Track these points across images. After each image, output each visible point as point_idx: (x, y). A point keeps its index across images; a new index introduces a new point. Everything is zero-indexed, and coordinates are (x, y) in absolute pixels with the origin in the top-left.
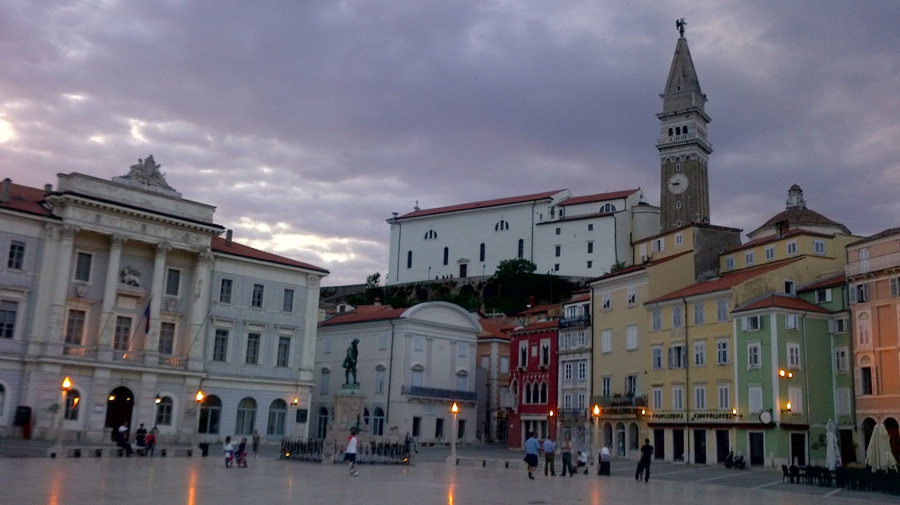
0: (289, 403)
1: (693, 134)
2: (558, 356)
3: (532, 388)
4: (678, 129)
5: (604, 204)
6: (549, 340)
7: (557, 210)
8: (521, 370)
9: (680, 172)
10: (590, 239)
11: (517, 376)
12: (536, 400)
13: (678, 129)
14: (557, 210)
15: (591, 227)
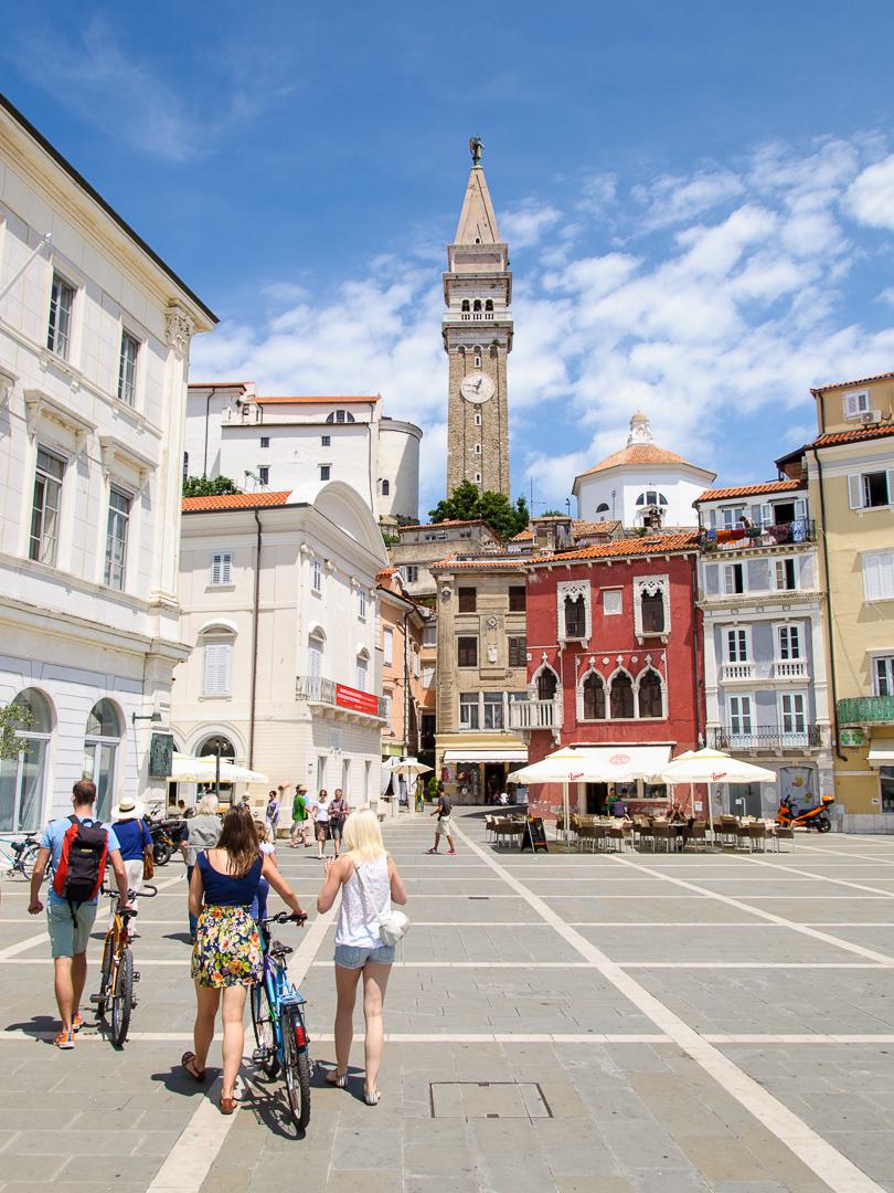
0: (127, 713)
1: (499, 315)
2: (697, 615)
3: (607, 686)
4: (477, 305)
5: (334, 409)
6: (666, 578)
7: (253, 408)
8: (573, 648)
9: (481, 369)
10: (325, 461)
11: (556, 663)
12: (623, 707)
13: (477, 305)
14: (253, 408)
15: (326, 441)
